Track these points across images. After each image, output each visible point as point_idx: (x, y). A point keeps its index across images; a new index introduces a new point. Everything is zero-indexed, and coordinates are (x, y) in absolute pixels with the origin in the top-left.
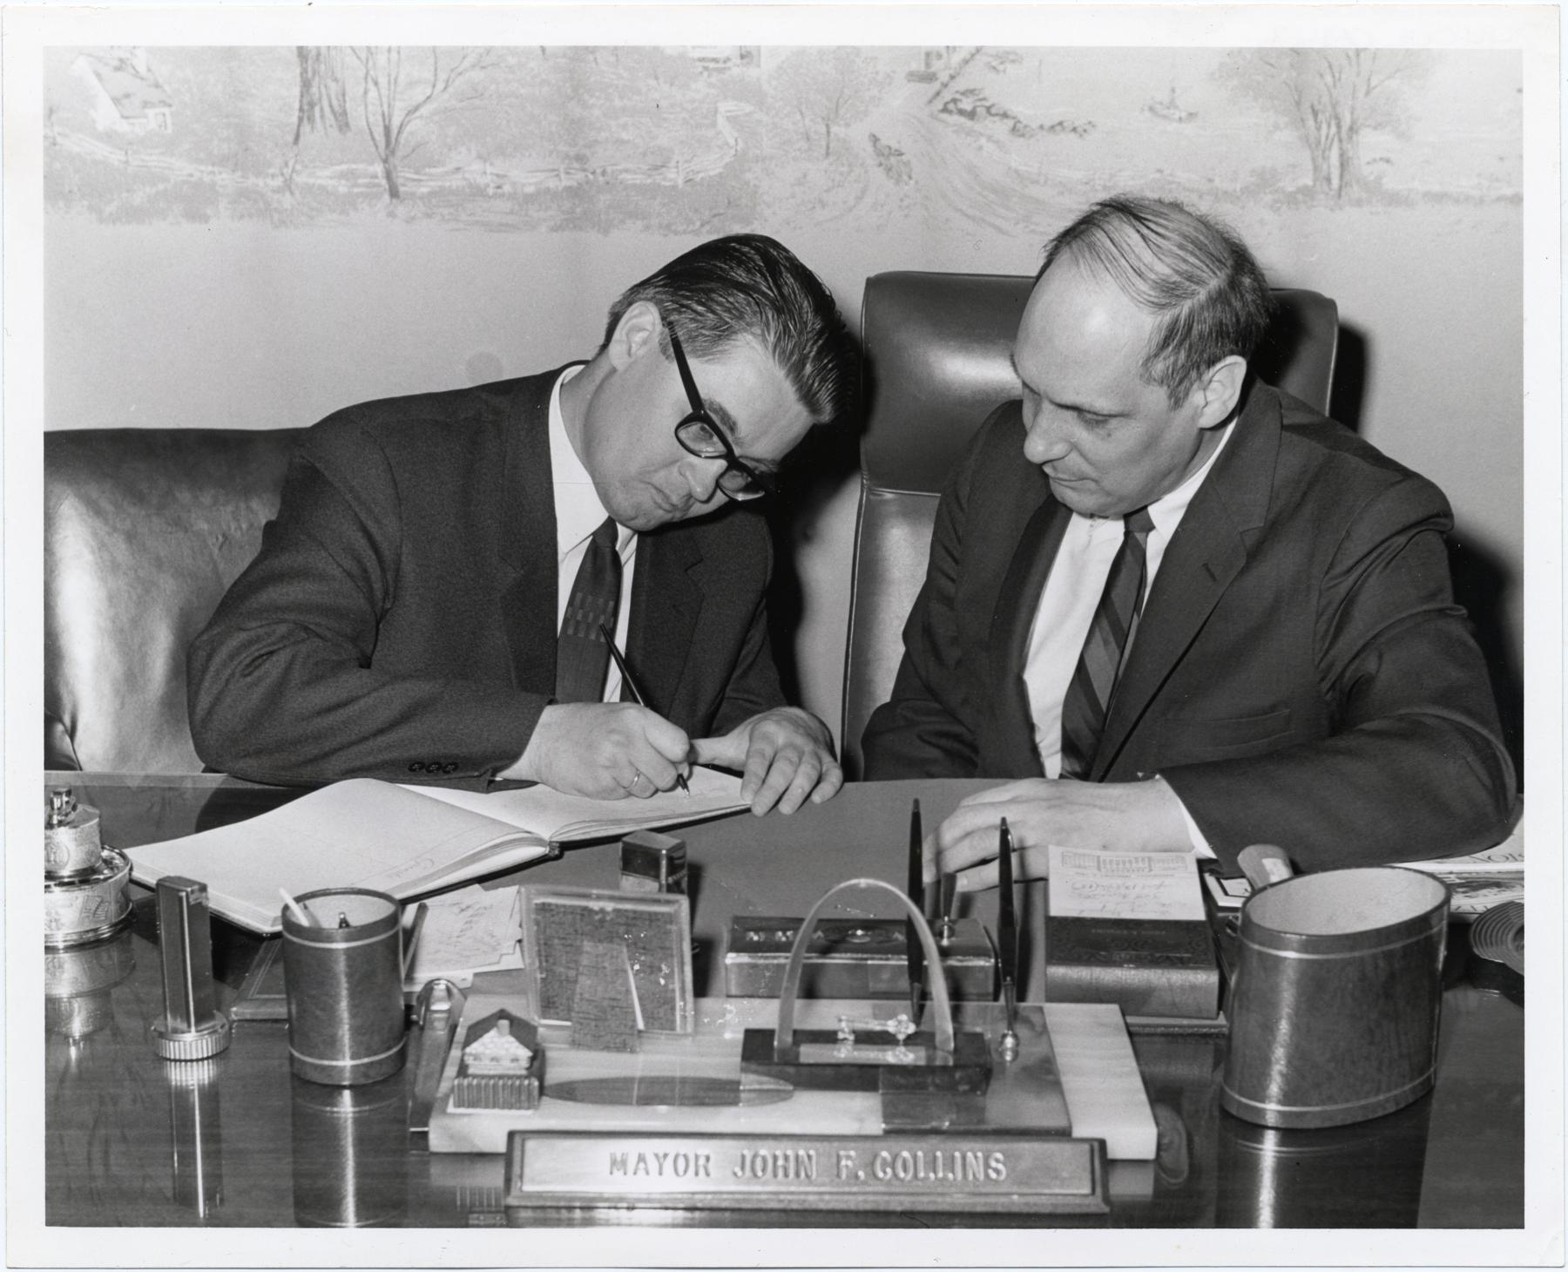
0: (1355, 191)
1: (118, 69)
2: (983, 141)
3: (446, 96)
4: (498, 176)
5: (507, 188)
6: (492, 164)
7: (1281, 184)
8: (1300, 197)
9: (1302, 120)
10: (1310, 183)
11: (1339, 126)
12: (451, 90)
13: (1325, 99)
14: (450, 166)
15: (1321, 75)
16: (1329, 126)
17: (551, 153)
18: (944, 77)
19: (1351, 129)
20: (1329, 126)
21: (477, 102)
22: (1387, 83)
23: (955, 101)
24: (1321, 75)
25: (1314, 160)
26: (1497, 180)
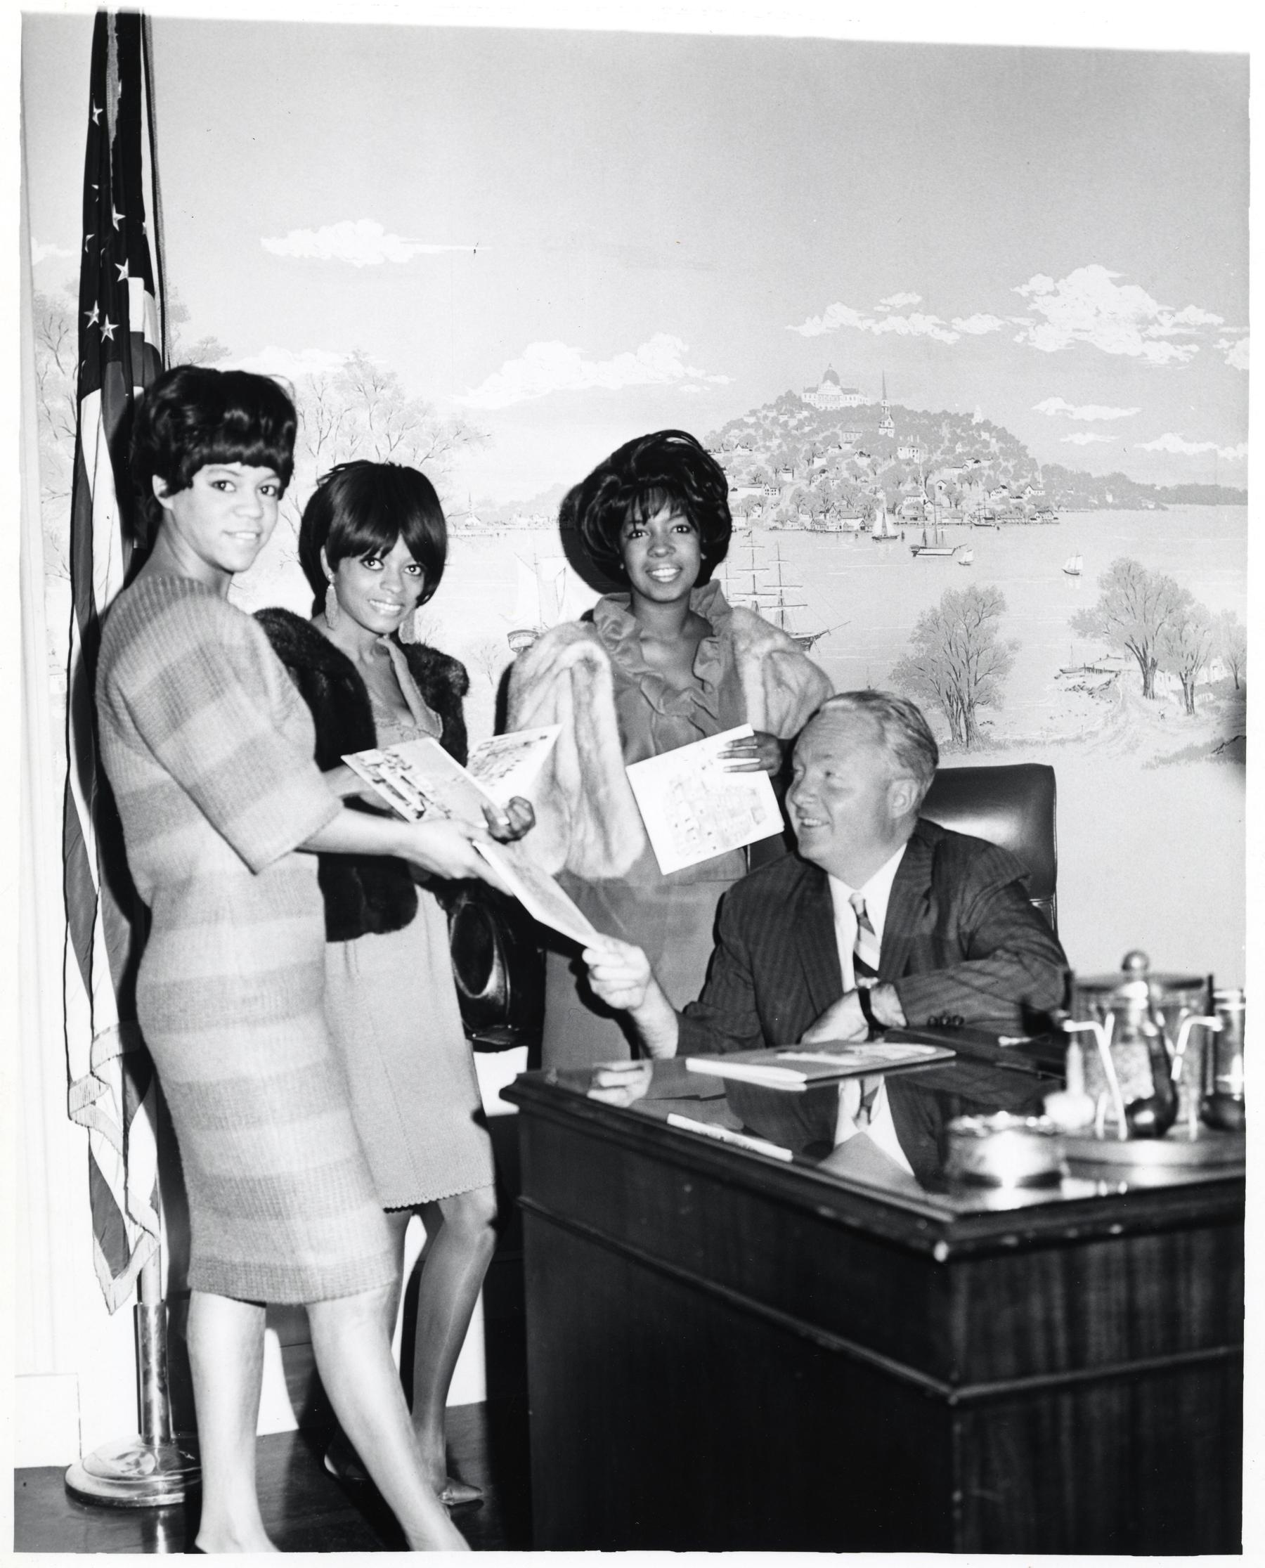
0: (976, 743)
8: (946, 748)
11: (963, 704)
13: (953, 688)
16: (957, 705)
19: (969, 705)
20: (957, 705)
22: (985, 677)
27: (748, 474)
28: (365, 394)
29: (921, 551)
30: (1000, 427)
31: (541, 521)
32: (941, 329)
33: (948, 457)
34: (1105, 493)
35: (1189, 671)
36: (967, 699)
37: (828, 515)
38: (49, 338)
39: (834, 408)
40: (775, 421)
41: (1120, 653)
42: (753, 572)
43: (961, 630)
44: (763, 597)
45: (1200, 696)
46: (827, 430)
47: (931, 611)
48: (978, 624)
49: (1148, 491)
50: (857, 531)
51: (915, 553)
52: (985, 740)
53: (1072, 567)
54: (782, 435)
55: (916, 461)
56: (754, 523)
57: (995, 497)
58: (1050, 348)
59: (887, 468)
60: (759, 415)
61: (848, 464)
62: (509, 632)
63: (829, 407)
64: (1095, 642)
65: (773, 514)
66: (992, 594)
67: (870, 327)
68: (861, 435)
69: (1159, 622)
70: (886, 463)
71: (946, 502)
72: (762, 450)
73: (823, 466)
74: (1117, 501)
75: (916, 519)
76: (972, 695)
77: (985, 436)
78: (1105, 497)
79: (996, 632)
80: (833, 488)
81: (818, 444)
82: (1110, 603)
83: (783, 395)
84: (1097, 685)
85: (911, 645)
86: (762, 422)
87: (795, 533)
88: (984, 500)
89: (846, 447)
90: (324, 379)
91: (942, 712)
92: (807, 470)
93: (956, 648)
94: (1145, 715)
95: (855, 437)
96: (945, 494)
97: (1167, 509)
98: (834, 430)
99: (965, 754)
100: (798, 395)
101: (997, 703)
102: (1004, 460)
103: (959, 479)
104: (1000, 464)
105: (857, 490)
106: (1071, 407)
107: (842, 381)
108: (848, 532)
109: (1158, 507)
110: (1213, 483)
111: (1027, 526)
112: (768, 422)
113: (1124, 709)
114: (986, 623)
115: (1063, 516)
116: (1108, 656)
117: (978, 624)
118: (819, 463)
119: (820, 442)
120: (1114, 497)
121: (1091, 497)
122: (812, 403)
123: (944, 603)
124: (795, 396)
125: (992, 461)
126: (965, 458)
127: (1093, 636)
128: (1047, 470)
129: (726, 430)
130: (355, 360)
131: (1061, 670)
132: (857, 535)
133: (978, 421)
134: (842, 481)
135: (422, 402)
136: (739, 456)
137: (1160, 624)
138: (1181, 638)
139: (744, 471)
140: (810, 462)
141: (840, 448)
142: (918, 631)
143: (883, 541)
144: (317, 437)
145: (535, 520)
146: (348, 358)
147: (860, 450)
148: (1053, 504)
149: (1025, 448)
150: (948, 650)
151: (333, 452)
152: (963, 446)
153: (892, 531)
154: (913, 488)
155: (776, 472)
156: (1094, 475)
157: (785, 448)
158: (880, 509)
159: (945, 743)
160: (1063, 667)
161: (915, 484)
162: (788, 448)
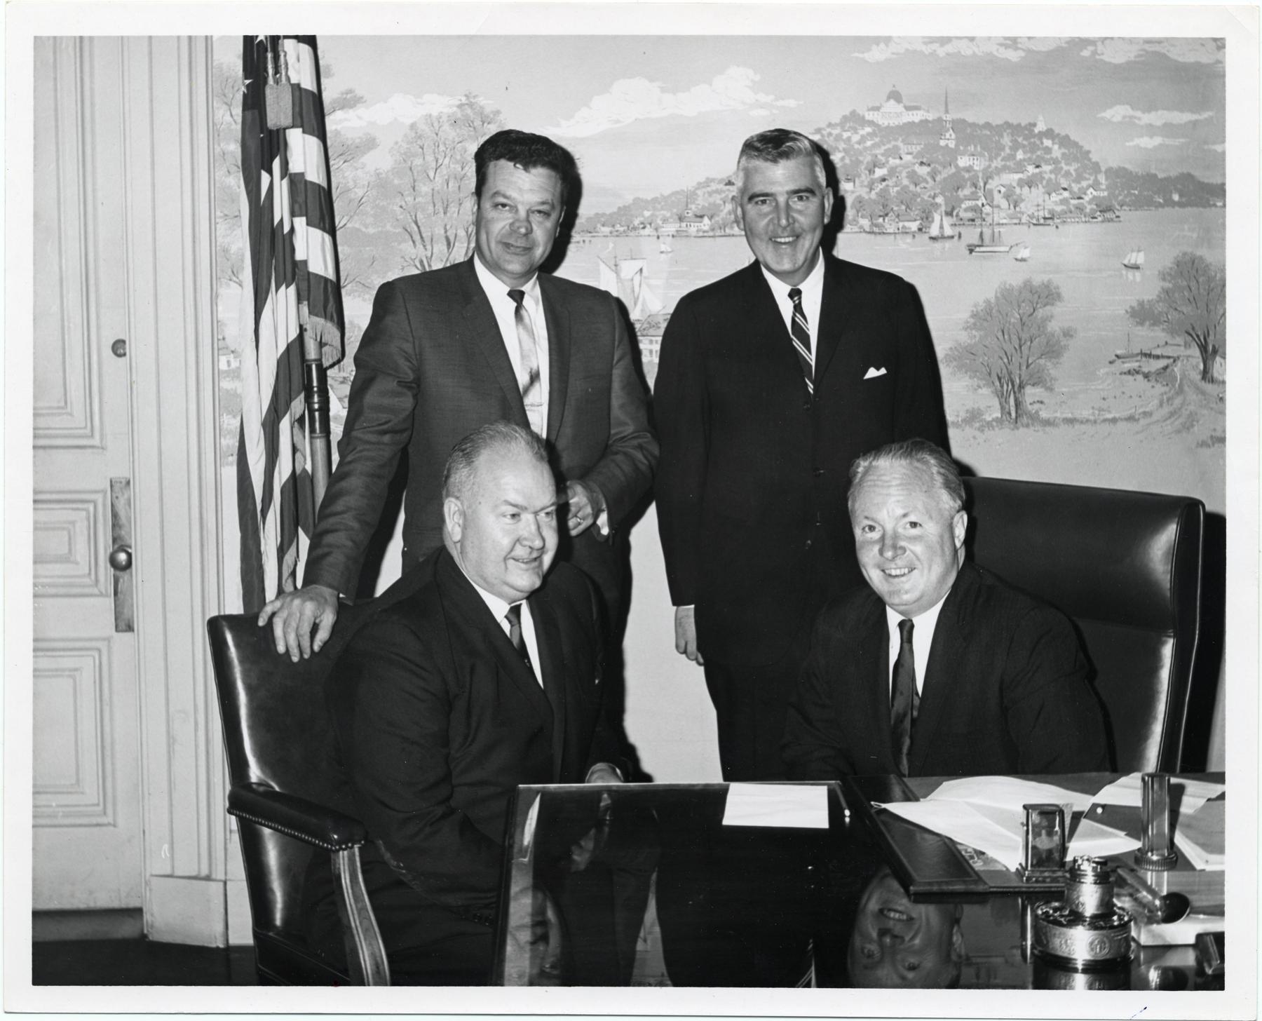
0: (1025, 420)
1: (342, 383)
7: (984, 417)
8: (994, 424)
9: (993, 383)
10: (999, 415)
13: (1005, 371)
15: (1002, 359)
16: (1008, 385)
20: (1008, 385)
24: (1002, 359)
25: (1000, 404)
26: (1103, 410)
28: (474, 128)
29: (978, 249)
30: (1063, 134)
31: (622, 229)
32: (1006, 48)
33: (1008, 163)
34: (1171, 192)
36: (1018, 381)
37: (886, 220)
38: (225, 96)
39: (897, 123)
41: (1179, 340)
43: (1014, 318)
46: (889, 142)
47: (985, 302)
48: (1032, 314)
50: (915, 232)
51: (971, 251)
52: (1035, 418)
53: (1133, 262)
54: (844, 150)
55: (976, 168)
57: (1055, 197)
58: (1120, 59)
59: (946, 175)
60: (824, 132)
61: (908, 172)
63: (891, 125)
64: (1152, 330)
66: (1047, 285)
67: (935, 51)
68: (922, 146)
70: (946, 171)
71: (1004, 204)
73: (885, 175)
74: (1184, 200)
76: (1022, 379)
77: (1047, 143)
78: (1171, 196)
79: (1050, 321)
80: (892, 194)
81: (879, 157)
82: (1171, 295)
83: (847, 113)
84: (1153, 370)
85: (964, 333)
86: (826, 139)
87: (855, 235)
88: (1044, 201)
89: (909, 158)
90: (441, 117)
91: (992, 392)
92: (869, 179)
94: (1203, 397)
95: (916, 149)
96: (1004, 197)
98: (896, 143)
99: (1013, 430)
100: (861, 113)
101: (1049, 384)
102: (1066, 164)
103: (1018, 185)
104: (1062, 168)
105: (916, 195)
106: (1139, 114)
107: (904, 101)
108: (907, 233)
111: (1088, 225)
112: (831, 138)
113: (1181, 391)
114: (1041, 313)
115: (1125, 214)
116: (1166, 343)
117: (1032, 314)
118: (879, 172)
120: (1181, 196)
121: (1156, 196)
122: (875, 120)
123: (999, 295)
124: (859, 115)
125: (1053, 166)
126: (1026, 164)
127: (1154, 324)
128: (1110, 172)
130: (466, 102)
131: (1117, 356)
132: (914, 236)
133: (1041, 129)
134: (902, 189)
140: (871, 172)
141: (901, 158)
142: (972, 321)
143: (940, 240)
144: (434, 165)
145: (617, 229)
146: (461, 100)
147: (921, 160)
149: (1089, 152)
150: (1001, 337)
151: (446, 177)
152: (1025, 153)
153: (948, 231)
154: (972, 193)
156: (1159, 177)
157: (847, 161)
158: (939, 211)
159: (993, 420)
160: (1119, 352)
161: (974, 189)
162: (851, 160)
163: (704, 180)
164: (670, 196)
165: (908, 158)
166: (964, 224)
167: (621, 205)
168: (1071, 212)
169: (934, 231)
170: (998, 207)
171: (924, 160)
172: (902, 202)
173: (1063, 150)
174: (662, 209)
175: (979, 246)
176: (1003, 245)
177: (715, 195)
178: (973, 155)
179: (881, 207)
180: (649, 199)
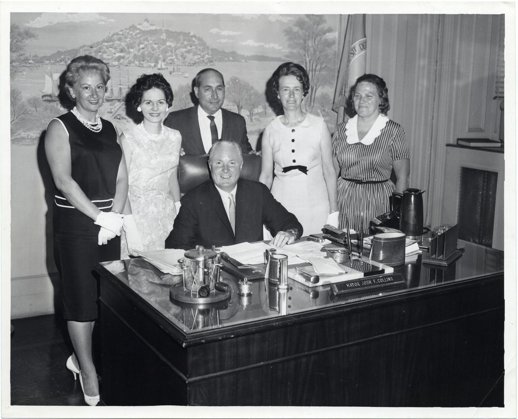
2: (122, 124)
3: (17, 120)
4: (28, 135)
5: (29, 137)
6: (26, 133)
12: (18, 119)
14: (17, 134)
17: (38, 130)
18: (114, 112)
21: (22, 121)
23: (116, 117)
27: (120, 49)
29: (173, 73)
30: (198, 36)
31: (53, 62)
33: (183, 45)
35: (252, 109)
37: (144, 62)
40: (128, 33)
41: (231, 104)
42: (120, 79)
44: (123, 86)
45: (255, 117)
49: (243, 57)
51: (171, 74)
55: (172, 46)
56: (121, 64)
57: (196, 57)
62: (43, 95)
63: (146, 30)
65: (127, 61)
69: (243, 95)
71: (181, 58)
72: (124, 42)
75: (171, 63)
77: (194, 39)
81: (142, 41)
83: (131, 25)
86: (124, 33)
89: (151, 42)
93: (182, 103)
97: (247, 62)
102: (200, 46)
105: (153, 54)
106: (220, 31)
109: (245, 61)
110: (261, 55)
118: (142, 46)
119: (143, 40)
129: (113, 36)
132: (153, 68)
135: (15, 25)
136: (117, 44)
137: (244, 96)
138: (250, 100)
139: (118, 48)
140: (139, 46)
141: (148, 42)
147: (154, 43)
148: (214, 60)
149: (206, 43)
152: (187, 42)
153: (164, 67)
154: (171, 54)
155: (128, 48)
161: (171, 53)
163: (82, 45)
164: (70, 51)
165: (151, 42)
166: (168, 65)
167: (53, 53)
168: (201, 62)
169: (159, 66)
170: (179, 59)
171: (156, 43)
172: (149, 57)
173: (199, 42)
174: (68, 55)
175: (173, 72)
176: (180, 72)
177: (86, 51)
178: (171, 42)
179: (142, 58)
180: (63, 51)
